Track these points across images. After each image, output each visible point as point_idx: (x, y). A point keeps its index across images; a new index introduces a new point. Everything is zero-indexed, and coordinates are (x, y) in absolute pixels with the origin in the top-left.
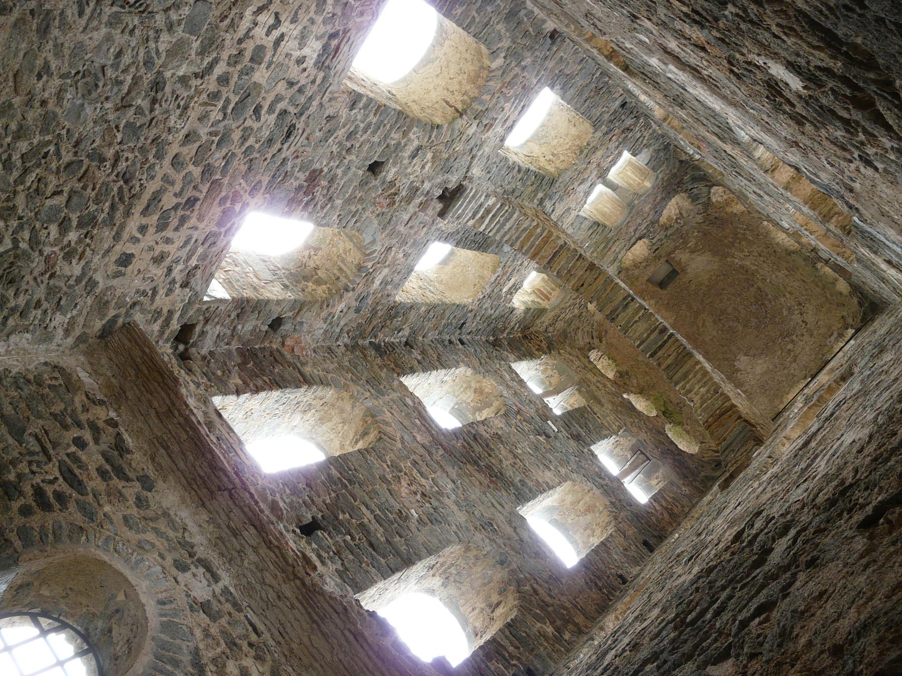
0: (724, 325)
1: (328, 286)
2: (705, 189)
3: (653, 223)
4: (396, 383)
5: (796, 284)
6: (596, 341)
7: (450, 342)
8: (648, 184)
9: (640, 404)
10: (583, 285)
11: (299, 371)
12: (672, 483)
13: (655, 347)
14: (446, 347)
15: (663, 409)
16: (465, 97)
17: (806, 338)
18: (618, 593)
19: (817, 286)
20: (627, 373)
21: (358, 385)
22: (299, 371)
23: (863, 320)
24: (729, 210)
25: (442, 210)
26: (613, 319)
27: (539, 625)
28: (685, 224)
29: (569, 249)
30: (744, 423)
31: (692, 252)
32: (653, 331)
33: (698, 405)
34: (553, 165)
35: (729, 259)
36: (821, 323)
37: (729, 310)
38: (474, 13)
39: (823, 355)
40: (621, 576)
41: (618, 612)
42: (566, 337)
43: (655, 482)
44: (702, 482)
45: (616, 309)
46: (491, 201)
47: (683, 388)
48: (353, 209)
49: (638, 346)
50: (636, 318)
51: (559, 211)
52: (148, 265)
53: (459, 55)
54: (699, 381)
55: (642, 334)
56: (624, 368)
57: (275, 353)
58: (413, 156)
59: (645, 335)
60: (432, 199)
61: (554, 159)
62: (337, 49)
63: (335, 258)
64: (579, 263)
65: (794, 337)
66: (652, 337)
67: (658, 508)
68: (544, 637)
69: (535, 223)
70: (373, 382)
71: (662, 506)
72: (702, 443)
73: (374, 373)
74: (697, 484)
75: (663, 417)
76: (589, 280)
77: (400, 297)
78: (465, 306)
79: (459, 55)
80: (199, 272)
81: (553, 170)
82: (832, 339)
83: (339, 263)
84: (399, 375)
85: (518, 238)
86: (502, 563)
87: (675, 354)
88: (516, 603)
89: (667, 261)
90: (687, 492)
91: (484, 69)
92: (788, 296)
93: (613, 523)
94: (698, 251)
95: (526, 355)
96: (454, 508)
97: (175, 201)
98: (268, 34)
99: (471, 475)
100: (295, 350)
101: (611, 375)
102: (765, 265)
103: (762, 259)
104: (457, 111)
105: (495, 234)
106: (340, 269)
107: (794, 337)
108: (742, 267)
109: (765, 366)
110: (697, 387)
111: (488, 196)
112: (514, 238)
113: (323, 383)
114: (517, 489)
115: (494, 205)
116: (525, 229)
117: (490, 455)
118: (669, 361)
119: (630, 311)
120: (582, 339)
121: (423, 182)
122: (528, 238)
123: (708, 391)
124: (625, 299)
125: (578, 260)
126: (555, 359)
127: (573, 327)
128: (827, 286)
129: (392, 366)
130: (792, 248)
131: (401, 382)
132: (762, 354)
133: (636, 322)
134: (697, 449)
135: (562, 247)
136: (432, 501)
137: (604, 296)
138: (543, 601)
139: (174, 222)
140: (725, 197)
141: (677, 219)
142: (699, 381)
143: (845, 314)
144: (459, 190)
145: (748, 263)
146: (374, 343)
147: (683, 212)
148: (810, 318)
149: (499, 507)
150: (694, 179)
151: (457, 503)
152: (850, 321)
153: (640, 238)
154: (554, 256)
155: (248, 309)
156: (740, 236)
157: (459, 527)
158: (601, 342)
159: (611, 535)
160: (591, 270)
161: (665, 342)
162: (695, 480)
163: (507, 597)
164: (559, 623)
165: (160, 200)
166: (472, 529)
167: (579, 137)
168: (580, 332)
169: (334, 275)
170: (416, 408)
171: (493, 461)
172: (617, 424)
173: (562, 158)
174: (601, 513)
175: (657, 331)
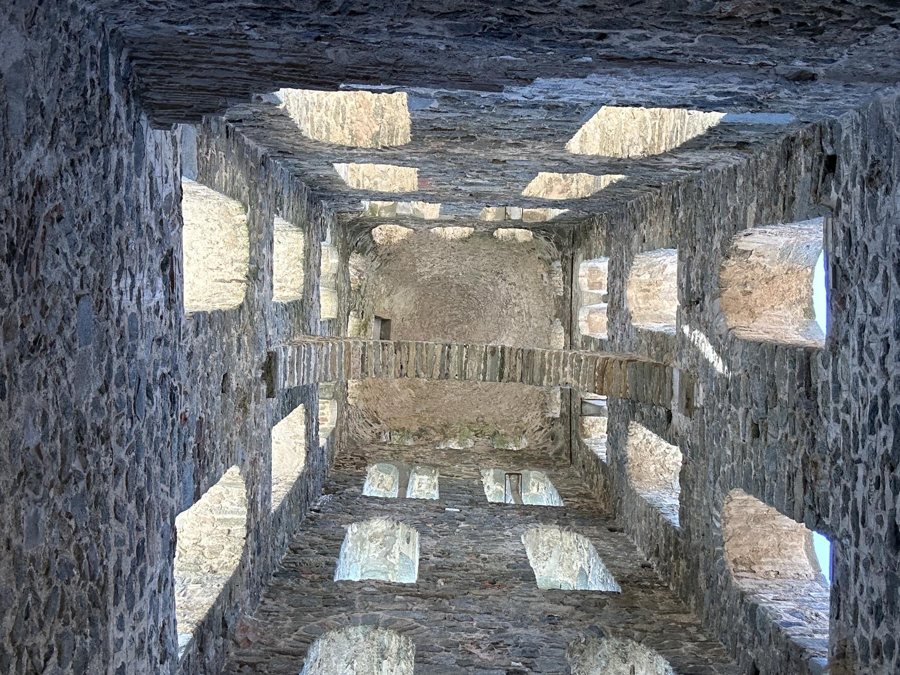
0: (452, 334)
1: (227, 547)
2: (367, 237)
3: (349, 293)
4: (341, 585)
5: (485, 260)
6: (376, 426)
7: (312, 519)
8: (336, 261)
9: (454, 445)
10: (402, 367)
11: (280, 653)
12: (551, 477)
13: (497, 369)
14: (314, 525)
15: (473, 433)
16: (236, 265)
17: (523, 294)
18: (661, 578)
19: (503, 249)
20: (421, 430)
21: (326, 615)
22: (280, 653)
23: (559, 247)
24: (395, 241)
25: (268, 389)
26: (447, 374)
27: (683, 650)
28: (368, 277)
29: (370, 346)
30: (631, 363)
31: (389, 295)
32: (485, 359)
33: (575, 382)
34: (287, 290)
35: (419, 280)
36: (525, 274)
37: (447, 319)
38: (224, 173)
39: (549, 296)
40: (643, 566)
41: (732, 572)
42: (355, 443)
43: (535, 488)
44: (560, 459)
45: (443, 365)
46: (290, 354)
47: (550, 379)
48: (226, 442)
49: (484, 380)
50: (464, 359)
51: (313, 328)
52: (135, 664)
53: (199, 230)
54: (558, 365)
55: (479, 367)
56: (415, 428)
57: (241, 659)
58: (239, 352)
59: (482, 366)
60: (259, 385)
61: (283, 284)
62: (172, 275)
63: (209, 516)
64: (386, 352)
65: (513, 301)
66: (489, 363)
67: (576, 500)
68: (698, 652)
69: (331, 345)
70: (329, 602)
71: (574, 497)
72: (524, 432)
73: (316, 594)
74: (558, 463)
75: (480, 439)
76: (404, 359)
77: (275, 505)
78: (303, 473)
79: (199, 230)
80: (166, 627)
81: (291, 294)
82: (545, 279)
83: (217, 517)
84: (332, 579)
85: (326, 369)
86: (601, 634)
87: (518, 361)
88: (648, 653)
89: (376, 317)
90: (566, 474)
91: (239, 226)
92: (484, 274)
93: (581, 537)
94: (392, 291)
95: (359, 481)
96: (521, 631)
97: (129, 559)
98: (131, 300)
99: (487, 597)
100: (250, 639)
101: (410, 442)
102: (451, 264)
103: (445, 261)
104: (241, 281)
105: (308, 380)
106: (223, 521)
107: (513, 301)
108: (433, 278)
109: (510, 338)
110: (560, 370)
111: (285, 349)
112: (323, 371)
113: (309, 641)
114: (517, 575)
115: (293, 353)
116: (327, 356)
117: (467, 570)
118: (519, 371)
119: (454, 358)
120: (366, 434)
121: (250, 371)
122: (333, 363)
123: (572, 366)
124: (443, 352)
125: (383, 349)
126: (373, 464)
127: (351, 429)
128: (511, 244)
129: (316, 577)
130: (466, 235)
131: (341, 581)
132: (500, 332)
133: (466, 362)
134: (524, 440)
135: (364, 349)
136: (506, 641)
137: (424, 362)
138: (655, 632)
139: (137, 587)
140: (384, 233)
141: (359, 277)
142: (558, 365)
143: (539, 255)
144: (272, 358)
145: (436, 272)
146: (279, 573)
147: (360, 268)
148: (514, 279)
149: (533, 599)
150: (354, 234)
151: (515, 625)
152: (548, 257)
153: (349, 314)
154: (363, 362)
155: (205, 631)
156: (416, 255)
157: (546, 640)
158: (379, 423)
159: (594, 545)
160: (400, 350)
161: (503, 358)
162: (555, 462)
163: (635, 657)
164: (683, 635)
165: (121, 572)
166: (552, 632)
167: (291, 250)
168: (360, 431)
169: (222, 532)
170: (380, 589)
171: (475, 572)
172: (472, 469)
173: (289, 279)
174: (561, 539)
175: (489, 356)
